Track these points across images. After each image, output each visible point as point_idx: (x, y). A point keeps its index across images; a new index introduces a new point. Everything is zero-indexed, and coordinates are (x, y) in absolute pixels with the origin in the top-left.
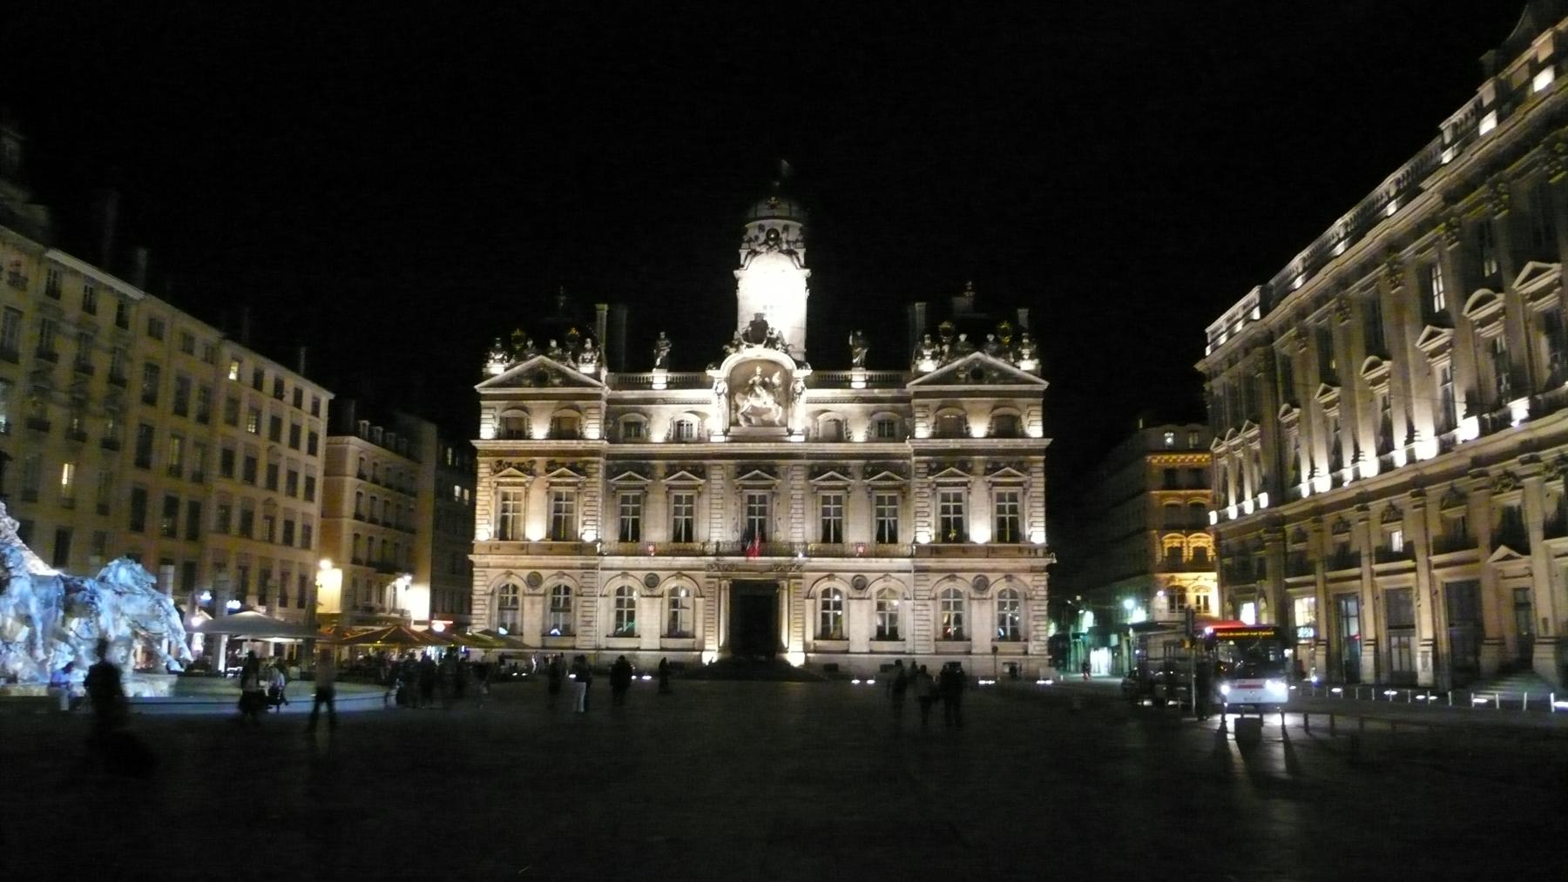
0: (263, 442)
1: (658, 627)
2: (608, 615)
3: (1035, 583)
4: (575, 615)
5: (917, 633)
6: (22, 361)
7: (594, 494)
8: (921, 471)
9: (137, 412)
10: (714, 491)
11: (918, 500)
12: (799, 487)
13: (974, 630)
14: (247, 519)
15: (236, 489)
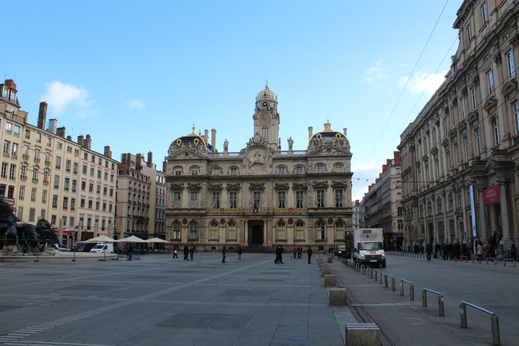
0: (95, 178)
1: (225, 236)
2: (209, 233)
3: (348, 220)
4: (198, 232)
5: (309, 237)
6: (18, 158)
7: (204, 193)
8: (310, 183)
9: (54, 172)
10: (243, 191)
11: (309, 193)
12: (271, 189)
13: (328, 236)
14: (90, 203)
15: (87, 194)
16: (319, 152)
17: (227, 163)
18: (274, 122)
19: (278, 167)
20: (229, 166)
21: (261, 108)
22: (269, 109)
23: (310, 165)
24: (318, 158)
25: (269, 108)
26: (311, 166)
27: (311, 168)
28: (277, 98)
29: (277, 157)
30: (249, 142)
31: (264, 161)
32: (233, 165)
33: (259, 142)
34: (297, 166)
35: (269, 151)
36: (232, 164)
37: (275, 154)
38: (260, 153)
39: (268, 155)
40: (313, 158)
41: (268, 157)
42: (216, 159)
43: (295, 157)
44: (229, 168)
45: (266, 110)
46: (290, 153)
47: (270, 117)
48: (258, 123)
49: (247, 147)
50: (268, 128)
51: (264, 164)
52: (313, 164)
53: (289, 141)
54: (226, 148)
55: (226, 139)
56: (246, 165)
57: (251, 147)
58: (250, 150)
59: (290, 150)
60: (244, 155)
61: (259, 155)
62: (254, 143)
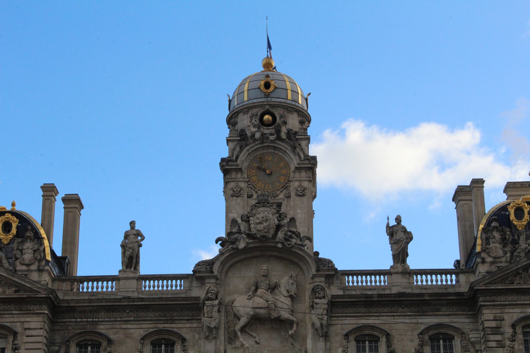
16: (524, 274)
17: (137, 320)
18: (306, 184)
19: (352, 338)
20: (142, 333)
21: (254, 130)
22: (283, 136)
23: (493, 324)
24: (522, 298)
25: (284, 130)
26: (497, 330)
27: (499, 337)
28: (306, 100)
29: (347, 293)
30: (229, 234)
31: (292, 312)
32: (161, 326)
33: (272, 231)
34: (431, 333)
35: (313, 271)
36: (158, 321)
37: (336, 282)
38: (274, 280)
39: (312, 286)
40: (503, 298)
41: (308, 294)
42: (90, 301)
43: (422, 295)
44: (143, 338)
45: (272, 138)
46: (398, 279)
47: (287, 166)
48: (243, 185)
49: (221, 253)
50: (279, 205)
51: (291, 323)
52: (503, 320)
53: (391, 231)
54: (131, 258)
55: (132, 224)
56: (217, 328)
57: (237, 252)
58: (231, 266)
59: (400, 268)
60: (210, 284)
61: (273, 288)
62: (250, 236)
